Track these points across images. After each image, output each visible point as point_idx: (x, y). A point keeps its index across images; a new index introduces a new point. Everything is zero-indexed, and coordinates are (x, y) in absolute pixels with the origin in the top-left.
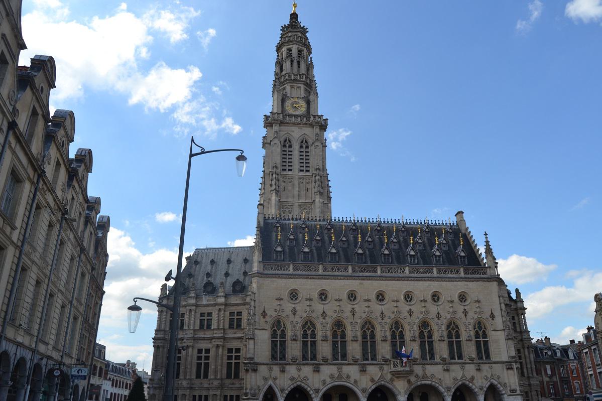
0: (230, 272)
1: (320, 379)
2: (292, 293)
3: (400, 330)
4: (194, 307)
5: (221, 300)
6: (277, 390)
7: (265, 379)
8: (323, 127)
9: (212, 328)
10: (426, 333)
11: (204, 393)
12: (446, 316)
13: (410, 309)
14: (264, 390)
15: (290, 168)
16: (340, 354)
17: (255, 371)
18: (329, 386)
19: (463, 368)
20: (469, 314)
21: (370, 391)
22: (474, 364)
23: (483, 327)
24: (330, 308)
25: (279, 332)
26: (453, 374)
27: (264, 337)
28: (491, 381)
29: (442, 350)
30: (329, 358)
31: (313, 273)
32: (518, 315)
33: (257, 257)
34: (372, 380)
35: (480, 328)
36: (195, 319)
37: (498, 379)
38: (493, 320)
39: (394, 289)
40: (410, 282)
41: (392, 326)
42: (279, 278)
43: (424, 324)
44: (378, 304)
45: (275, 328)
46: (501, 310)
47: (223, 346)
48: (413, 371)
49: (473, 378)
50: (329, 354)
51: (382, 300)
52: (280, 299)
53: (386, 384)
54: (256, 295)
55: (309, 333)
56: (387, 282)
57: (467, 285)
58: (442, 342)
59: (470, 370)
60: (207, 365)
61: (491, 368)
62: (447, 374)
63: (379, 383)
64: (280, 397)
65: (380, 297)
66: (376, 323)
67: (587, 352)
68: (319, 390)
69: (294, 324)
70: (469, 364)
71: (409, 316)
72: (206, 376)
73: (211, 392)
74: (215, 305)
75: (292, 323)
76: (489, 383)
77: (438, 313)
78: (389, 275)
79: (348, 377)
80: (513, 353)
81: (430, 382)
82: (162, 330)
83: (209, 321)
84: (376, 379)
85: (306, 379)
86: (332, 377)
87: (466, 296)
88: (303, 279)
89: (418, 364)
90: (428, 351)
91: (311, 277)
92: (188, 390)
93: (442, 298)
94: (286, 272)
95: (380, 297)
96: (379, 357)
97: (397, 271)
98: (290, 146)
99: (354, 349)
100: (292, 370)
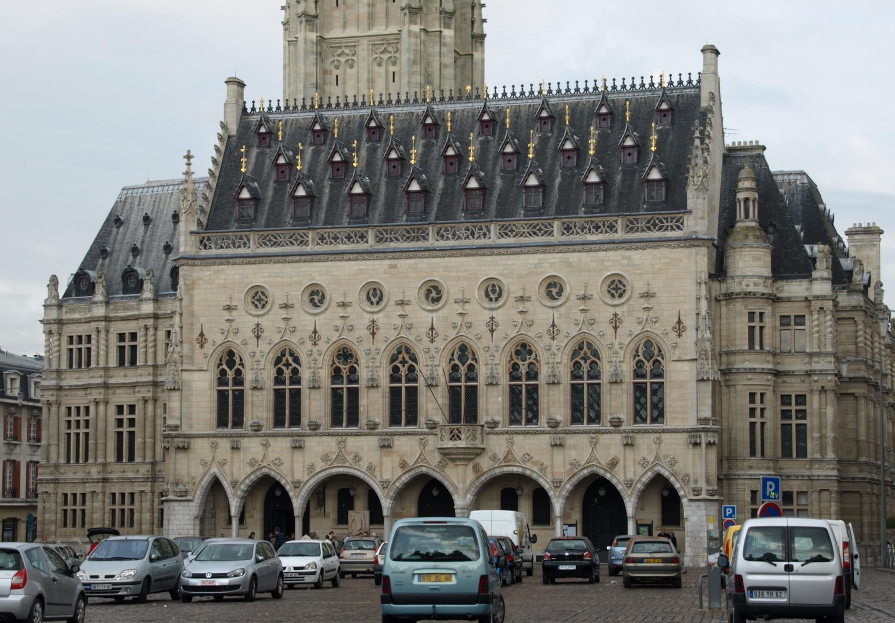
0: (174, 244)
1: (304, 463)
2: (257, 293)
3: (470, 361)
4: (103, 323)
5: (148, 308)
6: (226, 485)
7: (204, 464)
9: (138, 364)
10: (523, 369)
11: (127, 489)
12: (570, 330)
13: (492, 318)
14: (203, 483)
16: (345, 410)
17: (185, 449)
18: (322, 476)
19: (594, 444)
20: (624, 324)
21: (398, 484)
22: (619, 432)
23: (656, 352)
24: (327, 321)
25: (230, 374)
26: (573, 454)
27: (202, 387)
28: (656, 469)
29: (555, 403)
30: (323, 422)
31: (296, 249)
32: (811, 314)
33: (187, 225)
34: (403, 465)
36: (107, 347)
37: (672, 465)
38: (679, 335)
39: (460, 274)
40: (498, 257)
41: (453, 355)
42: (229, 264)
43: (523, 349)
44: (424, 309)
45: (225, 367)
46: (698, 314)
47: (155, 400)
48: (484, 449)
49: (613, 464)
50: (322, 414)
51: (437, 300)
52: (229, 308)
53: (431, 472)
54: (184, 303)
55: (287, 373)
56: (447, 259)
57: (629, 258)
58: (556, 387)
59: (610, 446)
60: (132, 435)
61: (659, 442)
62: (558, 454)
63: (418, 471)
65: (434, 294)
66: (418, 351)
68: (300, 483)
69: (258, 355)
70: (609, 432)
71: (489, 333)
72: (131, 458)
73: (137, 488)
74: (137, 318)
75: (253, 355)
76: (650, 474)
77: (553, 325)
78: (452, 243)
79: (357, 458)
80: (707, 413)
81: (520, 470)
82: (52, 371)
83: (134, 348)
84: (411, 462)
85: (278, 462)
86: (325, 458)
87: (624, 282)
88: (275, 263)
89: (497, 433)
90: (524, 405)
91: (291, 258)
92: (100, 484)
93: (567, 290)
94: (242, 251)
95: (434, 294)
96: (422, 419)
97: (473, 234)
99: (374, 404)
100: (253, 447)
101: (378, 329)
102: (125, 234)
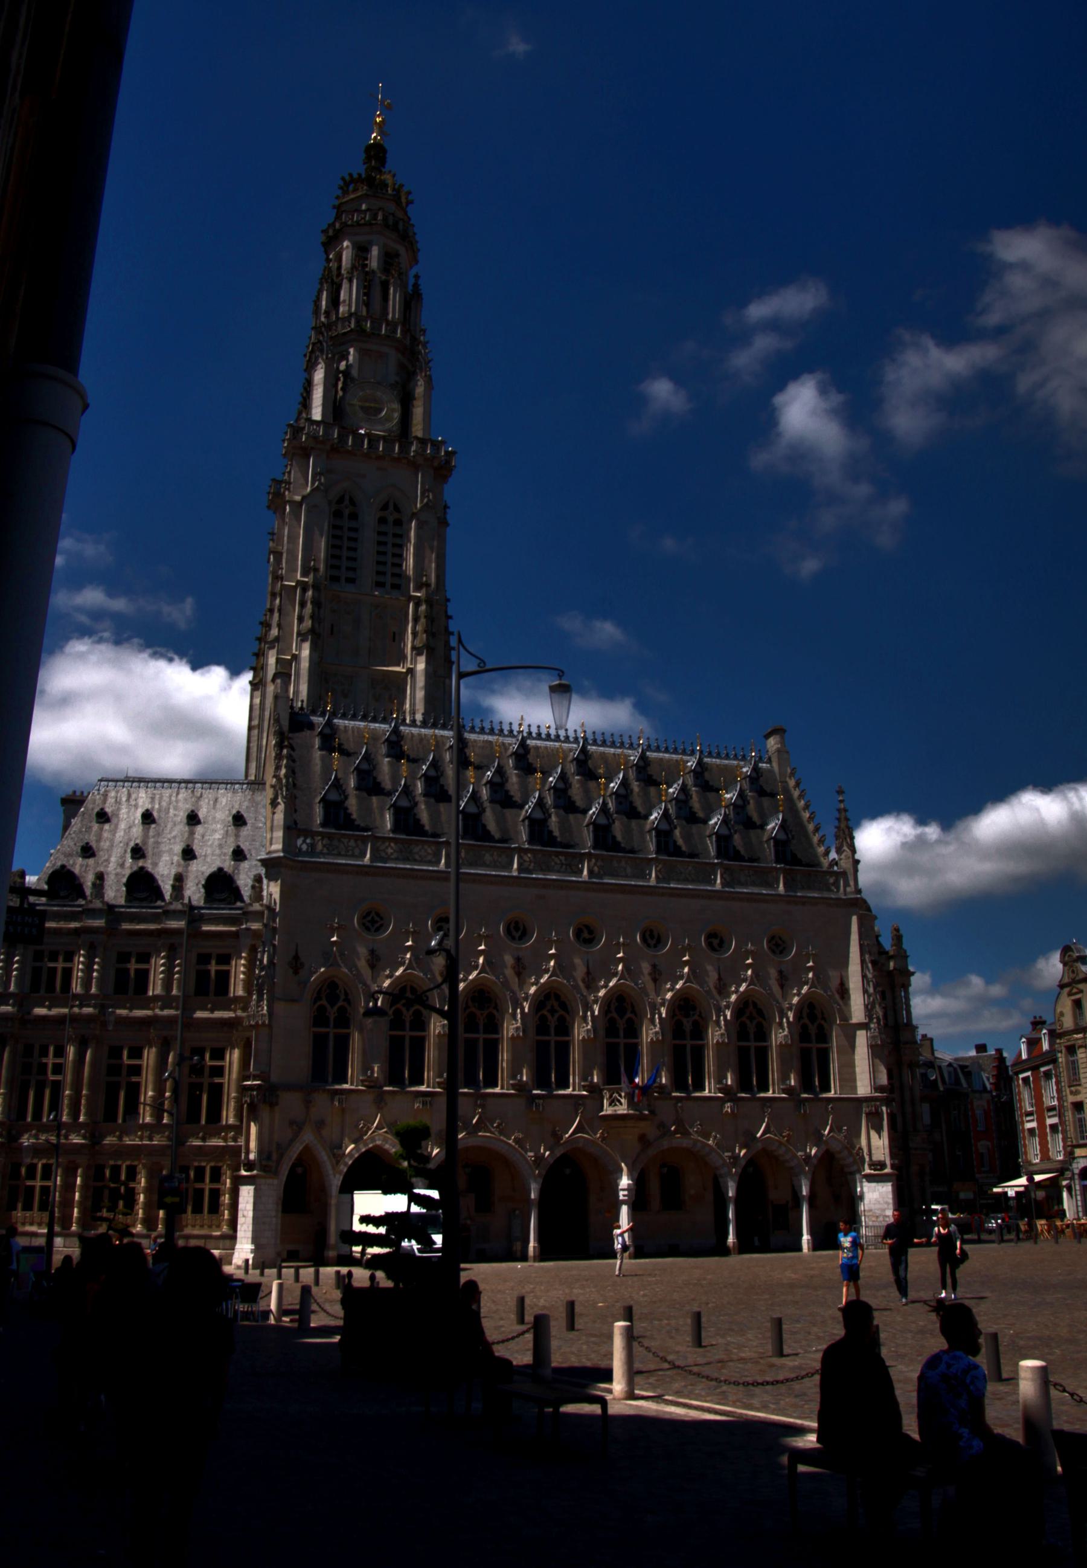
8: (441, 470)
10: (687, 1025)
15: (351, 575)
35: (812, 1017)
45: (324, 1002)
64: (331, 1172)
65: (586, 935)
67: (1028, 1077)
95: (586, 935)
98: (354, 516)
101: (524, 968)
102: (114, 832)
